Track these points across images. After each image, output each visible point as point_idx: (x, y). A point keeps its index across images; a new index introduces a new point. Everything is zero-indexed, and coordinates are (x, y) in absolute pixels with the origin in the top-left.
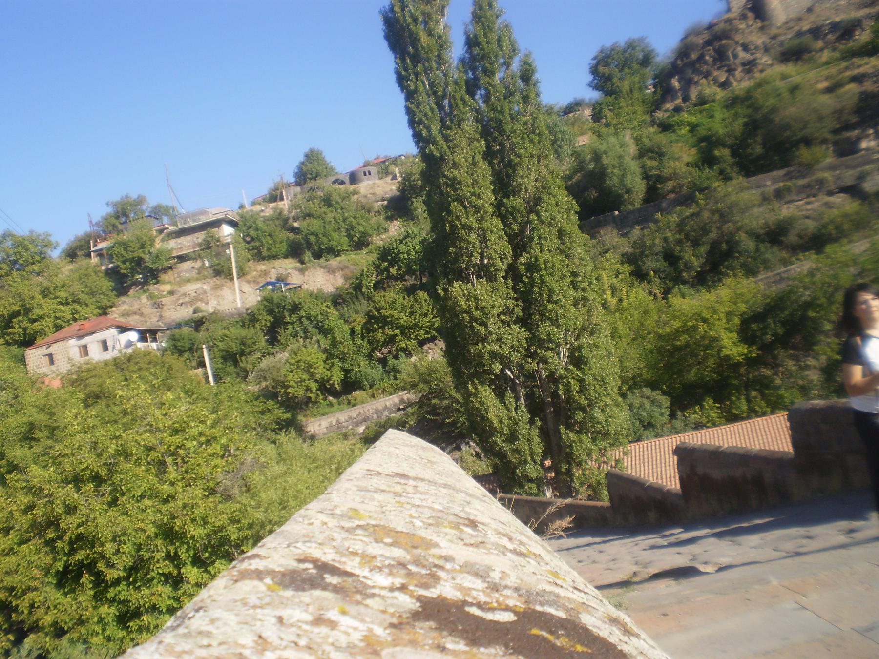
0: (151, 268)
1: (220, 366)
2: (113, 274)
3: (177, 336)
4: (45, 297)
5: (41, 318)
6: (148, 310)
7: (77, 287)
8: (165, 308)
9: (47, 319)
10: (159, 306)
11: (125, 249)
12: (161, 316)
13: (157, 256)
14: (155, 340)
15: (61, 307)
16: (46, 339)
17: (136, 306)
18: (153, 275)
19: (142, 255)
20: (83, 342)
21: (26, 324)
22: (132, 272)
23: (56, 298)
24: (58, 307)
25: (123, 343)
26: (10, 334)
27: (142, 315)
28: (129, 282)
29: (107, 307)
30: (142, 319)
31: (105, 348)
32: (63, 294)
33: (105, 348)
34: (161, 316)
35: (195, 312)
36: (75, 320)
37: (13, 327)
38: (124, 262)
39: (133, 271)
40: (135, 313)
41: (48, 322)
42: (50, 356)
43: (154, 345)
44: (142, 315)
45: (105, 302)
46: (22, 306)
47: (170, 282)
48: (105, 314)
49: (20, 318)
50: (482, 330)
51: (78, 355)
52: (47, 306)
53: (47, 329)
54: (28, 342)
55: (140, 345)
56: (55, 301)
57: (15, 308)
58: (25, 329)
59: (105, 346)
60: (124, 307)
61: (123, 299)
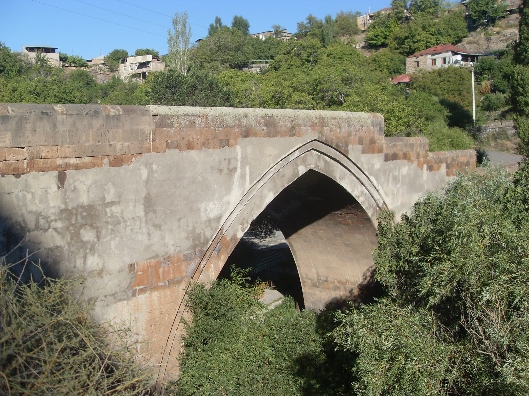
0: (492, 17)
1: (499, 80)
2: (468, 18)
3: (484, 61)
4: (423, 30)
5: (420, 41)
6: (483, 42)
7: (442, 27)
8: (492, 41)
9: (422, 42)
10: (488, 40)
11: (476, 5)
12: (488, 46)
13: (496, 10)
14: (472, 61)
15: (431, 37)
16: (420, 53)
17: (475, 40)
18: (492, 21)
19: (486, 10)
20: (434, 57)
21: (411, 44)
22: (479, 19)
23: (429, 31)
24: (429, 36)
25: (454, 60)
26: (402, 48)
27: (478, 44)
28: (477, 24)
29: (462, 37)
30: (478, 46)
31: (445, 62)
32: (433, 29)
33: (445, 62)
34: (488, 46)
35: (507, 47)
36: (437, 44)
37: (404, 44)
38: (475, 12)
39: (480, 18)
40: (475, 43)
41: (423, 44)
42: (418, 62)
43: (472, 63)
44: (478, 44)
45: (461, 34)
46: (410, 34)
47: (500, 27)
48: (459, 41)
49: (409, 40)
50: (521, 90)
51: (431, 64)
52: (424, 34)
53: (421, 48)
54: (410, 53)
55: (462, 63)
56: (428, 33)
57: (407, 34)
58: (410, 46)
59: (445, 59)
60: (471, 38)
61: (472, 33)
